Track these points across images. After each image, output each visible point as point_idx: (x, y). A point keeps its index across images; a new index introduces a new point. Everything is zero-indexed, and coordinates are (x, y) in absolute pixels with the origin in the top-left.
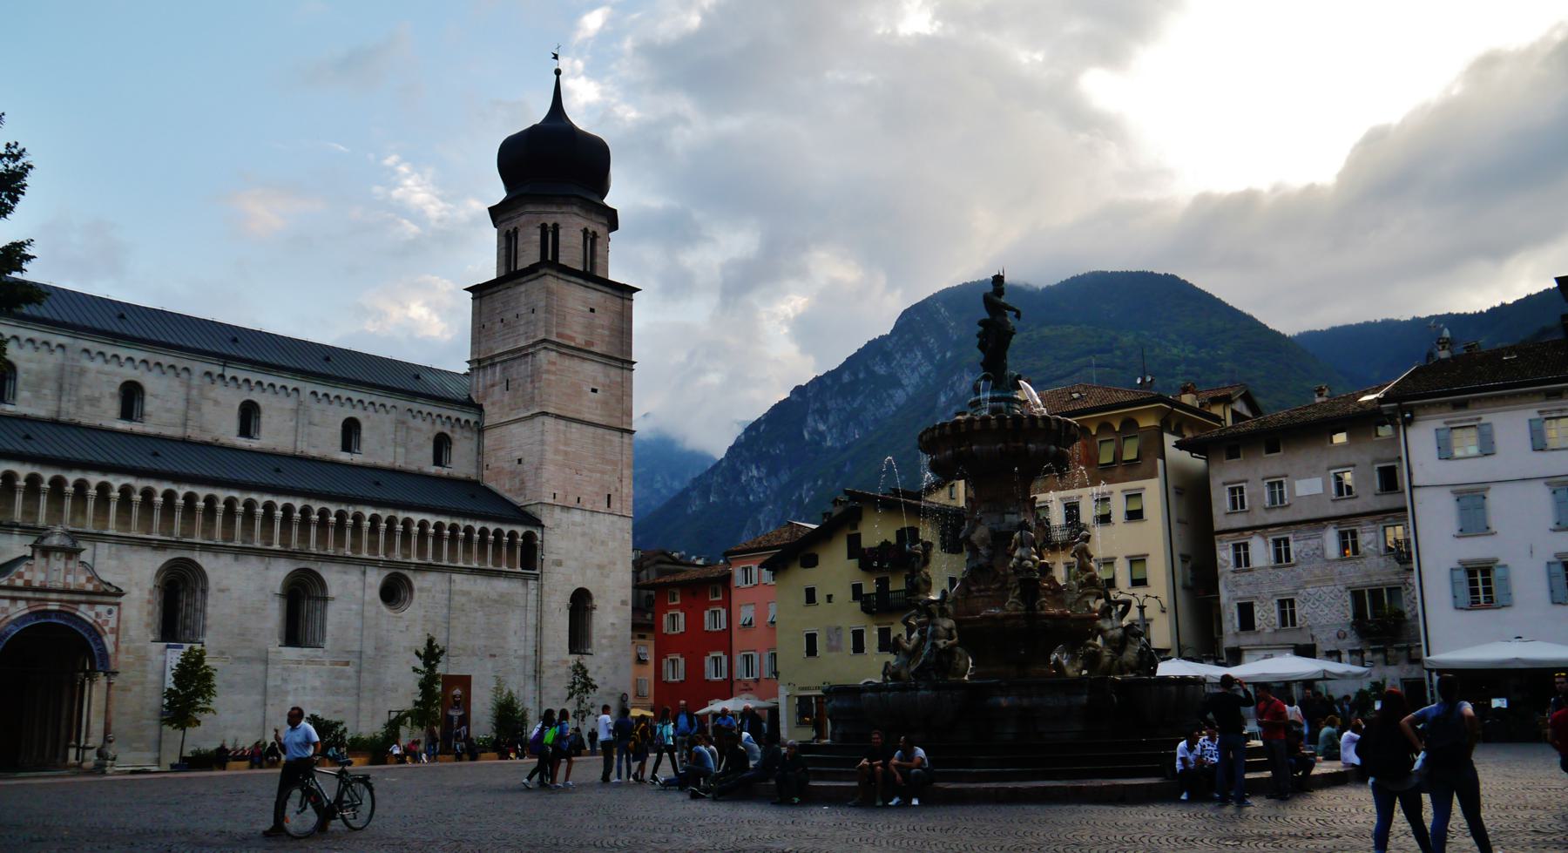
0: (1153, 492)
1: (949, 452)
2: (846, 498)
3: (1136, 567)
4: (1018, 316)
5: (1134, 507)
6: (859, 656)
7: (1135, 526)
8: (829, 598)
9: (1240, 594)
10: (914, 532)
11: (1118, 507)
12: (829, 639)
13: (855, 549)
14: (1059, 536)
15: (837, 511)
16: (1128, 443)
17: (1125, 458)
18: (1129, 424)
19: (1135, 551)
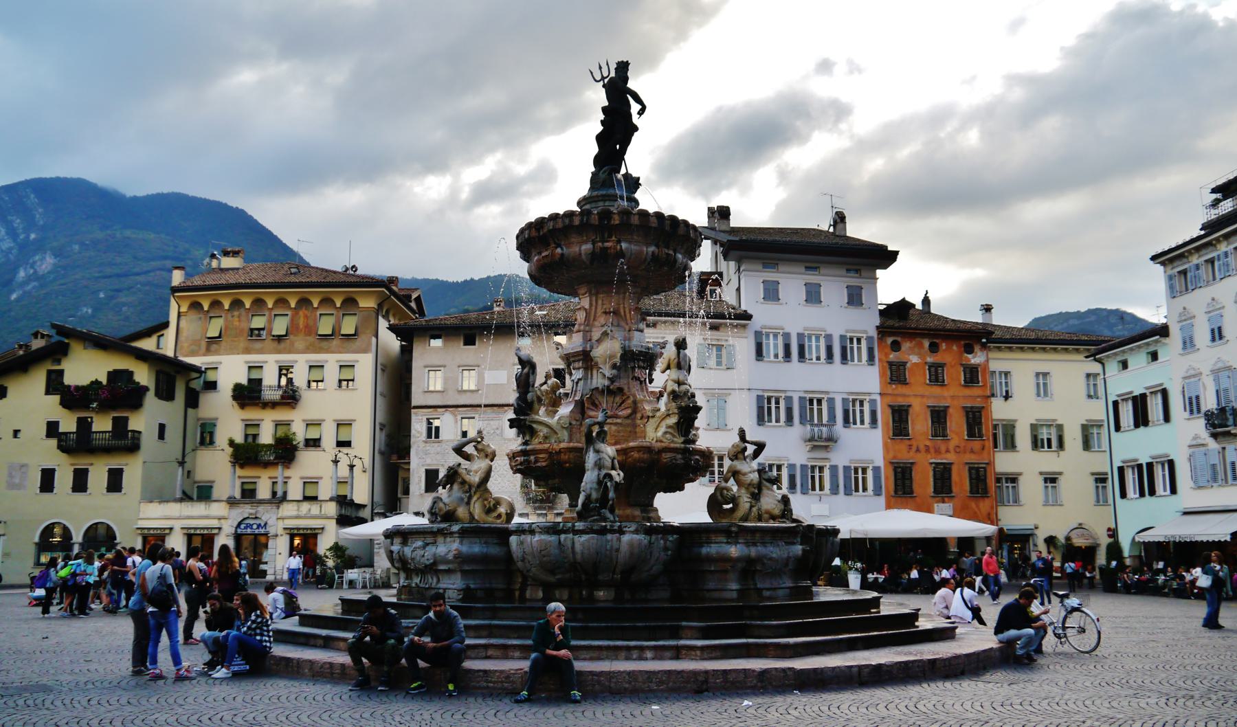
0: (365, 365)
1: (587, 247)
2: (53, 332)
3: (342, 429)
4: (641, 112)
5: (346, 374)
6: (47, 496)
7: (343, 394)
8: (16, 433)
9: (429, 461)
10: (131, 374)
11: (331, 373)
12: (10, 475)
13: (55, 384)
14: (269, 394)
15: (37, 344)
16: (346, 318)
17: (343, 332)
18: (350, 302)
19: (344, 416)
